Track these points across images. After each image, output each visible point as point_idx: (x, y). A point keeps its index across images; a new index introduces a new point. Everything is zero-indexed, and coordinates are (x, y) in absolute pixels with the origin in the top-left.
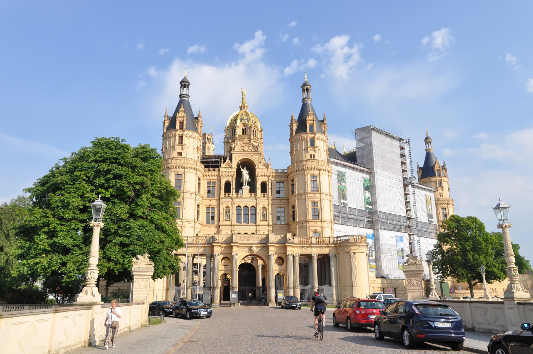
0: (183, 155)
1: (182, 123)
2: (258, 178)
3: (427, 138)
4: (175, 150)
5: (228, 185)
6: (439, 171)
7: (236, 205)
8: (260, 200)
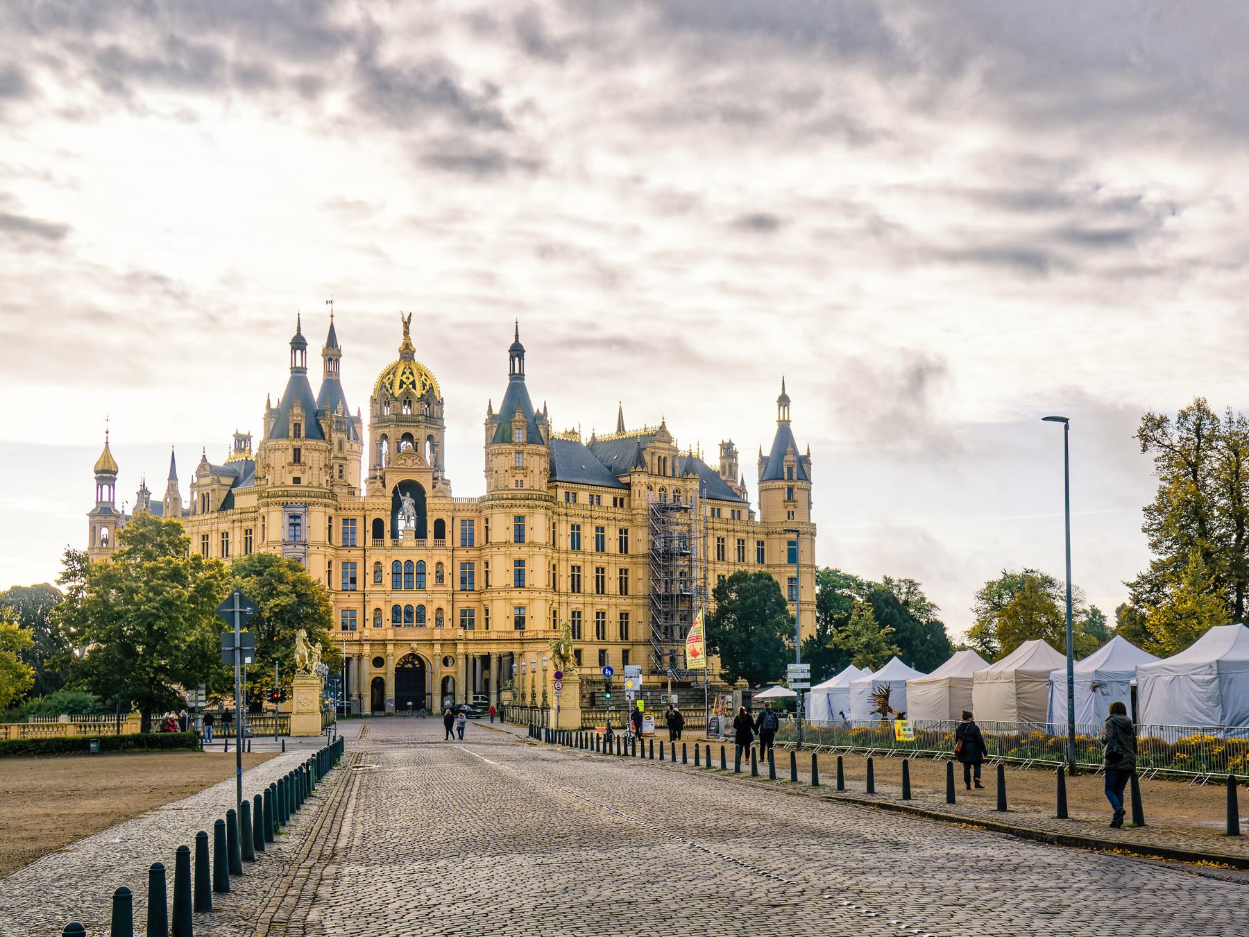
0: (304, 482)
5: (378, 524)
7: (394, 558)
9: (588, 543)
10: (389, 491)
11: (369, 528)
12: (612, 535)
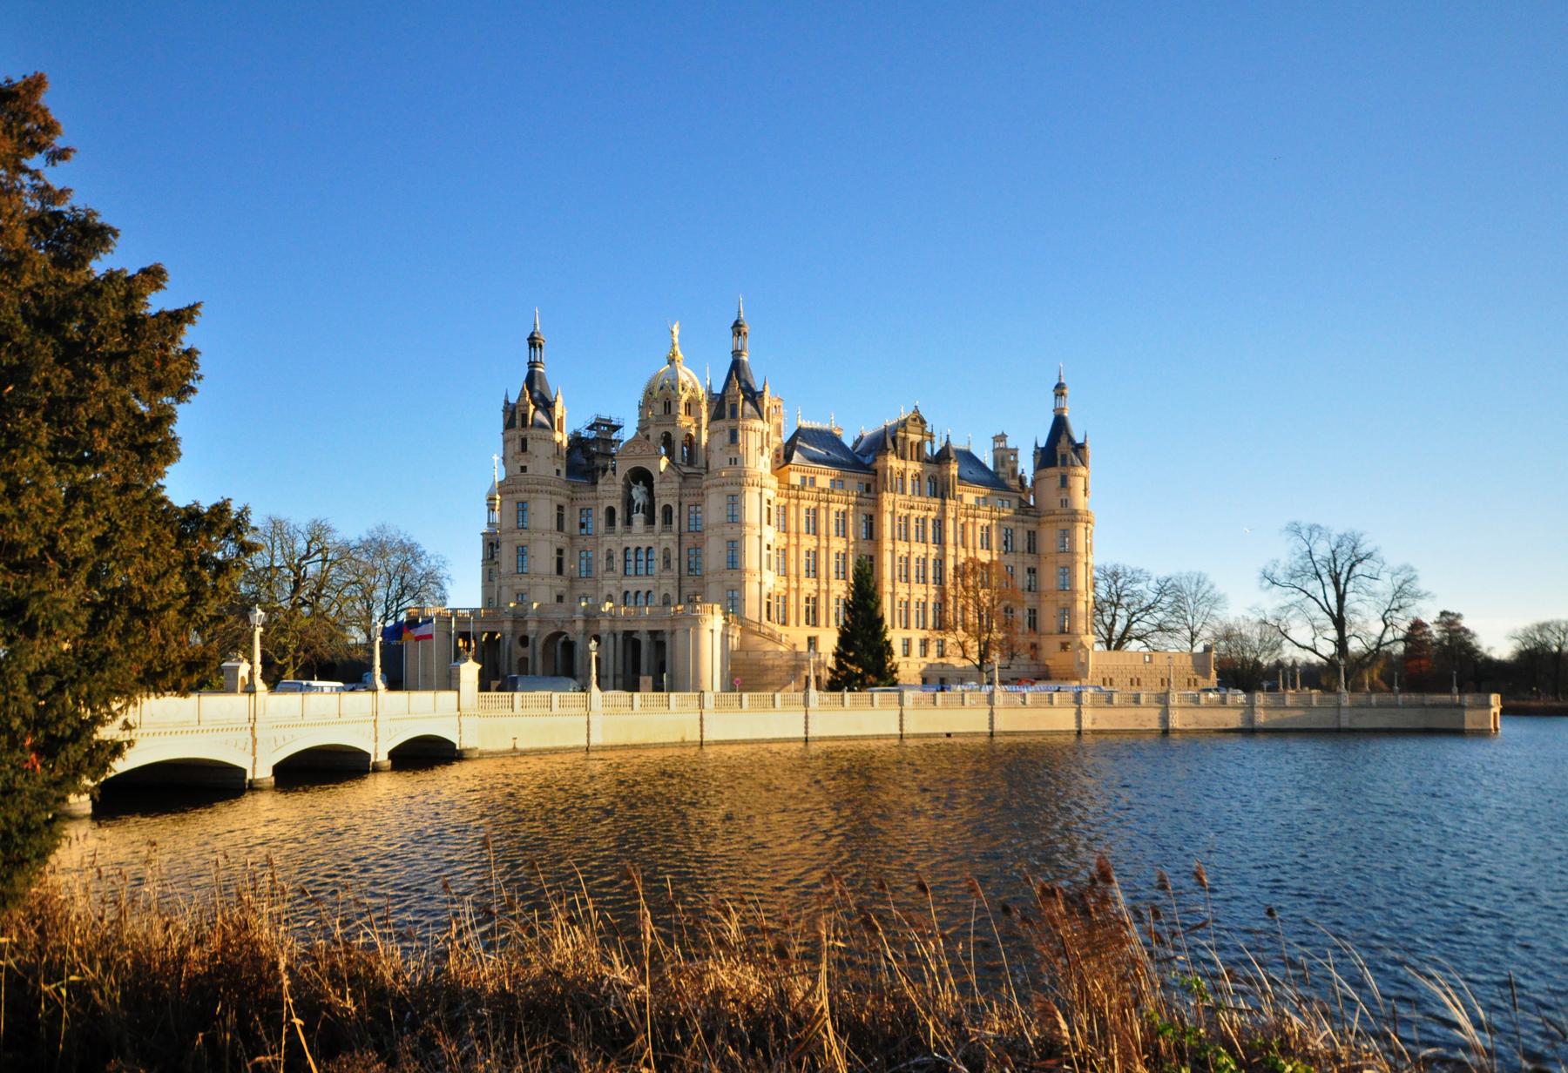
0: (529, 471)
5: (611, 512)
10: (620, 478)
11: (602, 515)
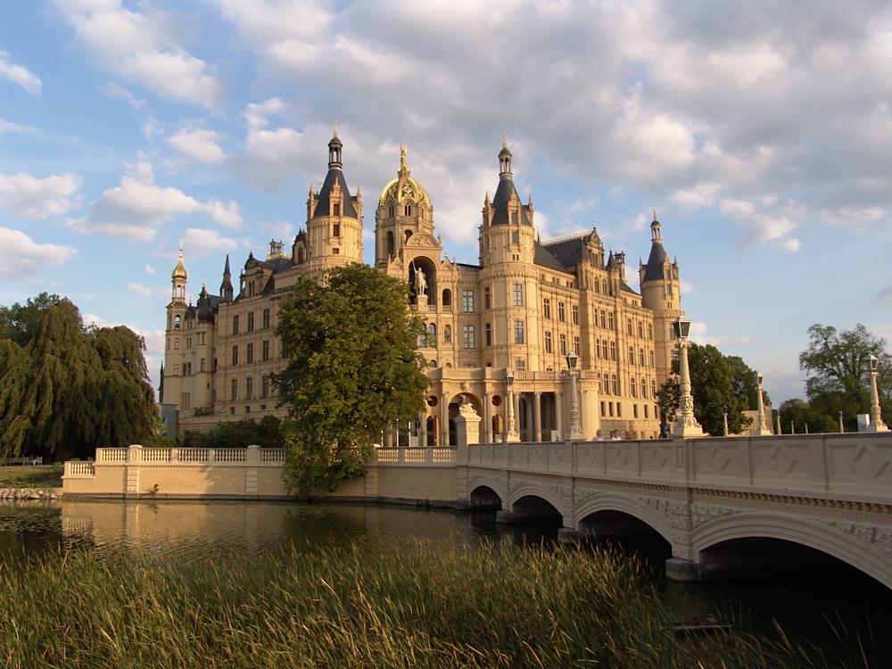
1: (337, 206)
2: (438, 284)
3: (655, 223)
4: (329, 244)
6: (669, 272)
8: (442, 316)
9: (555, 314)
10: (406, 266)
12: (569, 310)
